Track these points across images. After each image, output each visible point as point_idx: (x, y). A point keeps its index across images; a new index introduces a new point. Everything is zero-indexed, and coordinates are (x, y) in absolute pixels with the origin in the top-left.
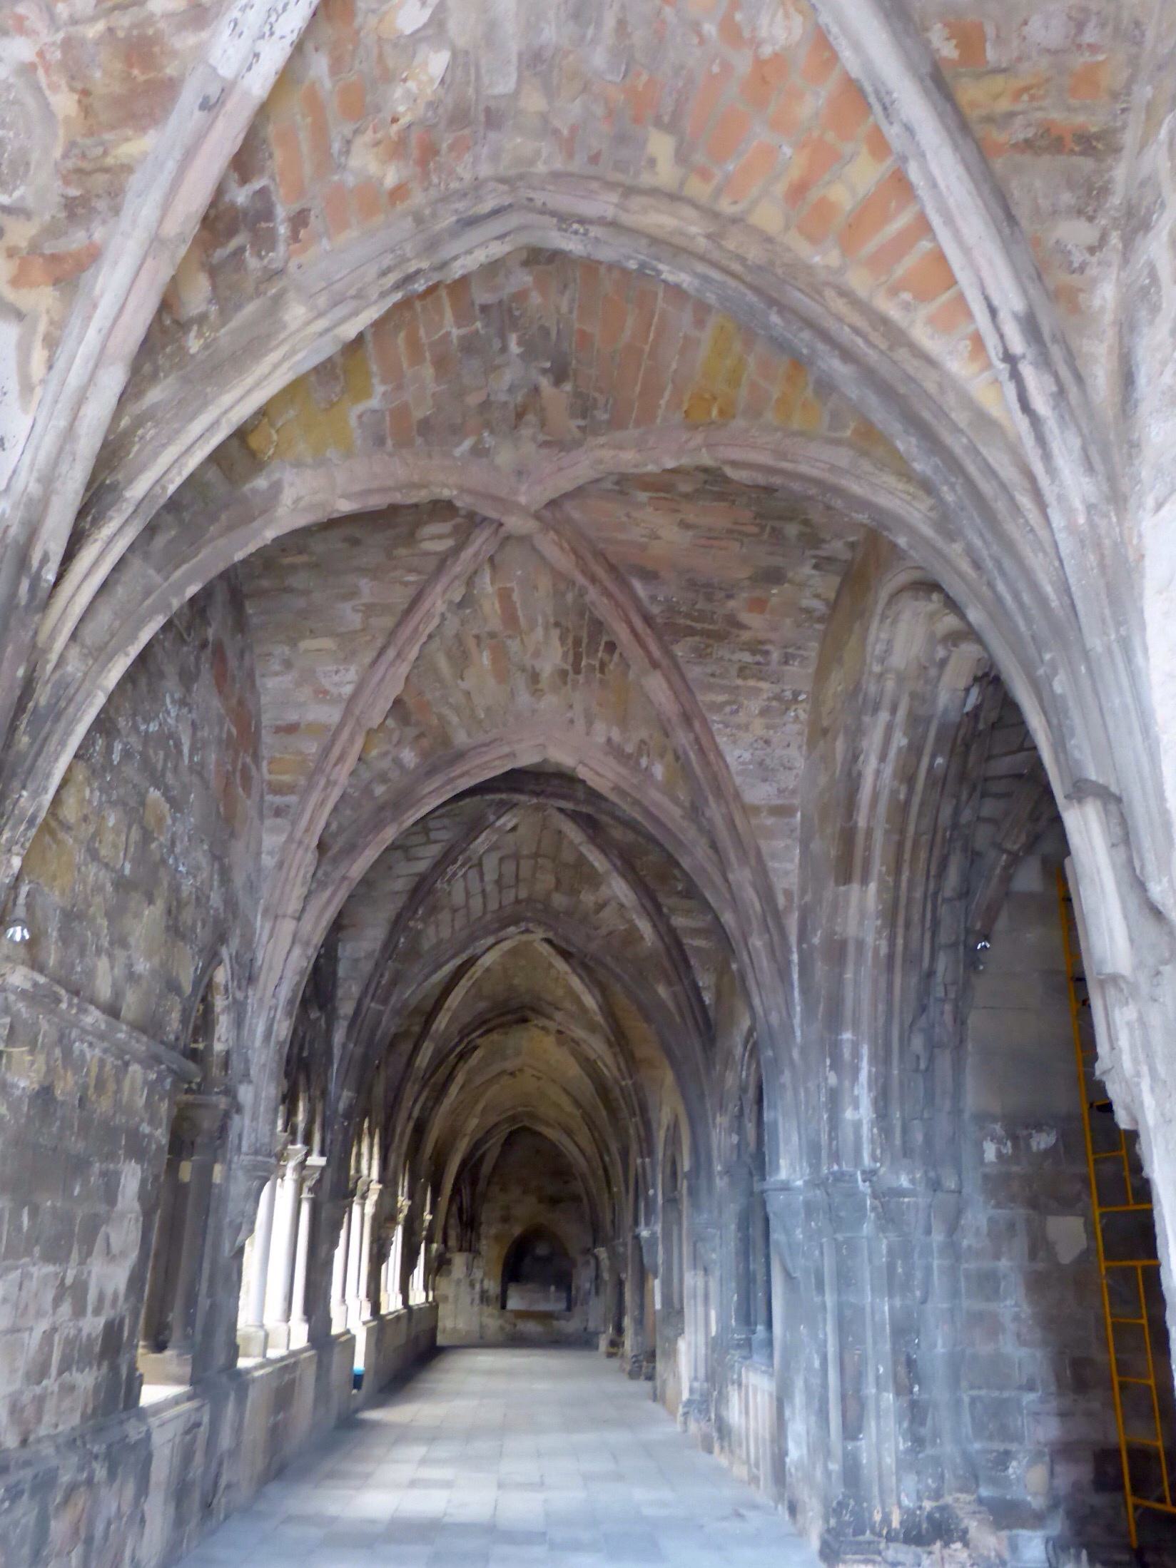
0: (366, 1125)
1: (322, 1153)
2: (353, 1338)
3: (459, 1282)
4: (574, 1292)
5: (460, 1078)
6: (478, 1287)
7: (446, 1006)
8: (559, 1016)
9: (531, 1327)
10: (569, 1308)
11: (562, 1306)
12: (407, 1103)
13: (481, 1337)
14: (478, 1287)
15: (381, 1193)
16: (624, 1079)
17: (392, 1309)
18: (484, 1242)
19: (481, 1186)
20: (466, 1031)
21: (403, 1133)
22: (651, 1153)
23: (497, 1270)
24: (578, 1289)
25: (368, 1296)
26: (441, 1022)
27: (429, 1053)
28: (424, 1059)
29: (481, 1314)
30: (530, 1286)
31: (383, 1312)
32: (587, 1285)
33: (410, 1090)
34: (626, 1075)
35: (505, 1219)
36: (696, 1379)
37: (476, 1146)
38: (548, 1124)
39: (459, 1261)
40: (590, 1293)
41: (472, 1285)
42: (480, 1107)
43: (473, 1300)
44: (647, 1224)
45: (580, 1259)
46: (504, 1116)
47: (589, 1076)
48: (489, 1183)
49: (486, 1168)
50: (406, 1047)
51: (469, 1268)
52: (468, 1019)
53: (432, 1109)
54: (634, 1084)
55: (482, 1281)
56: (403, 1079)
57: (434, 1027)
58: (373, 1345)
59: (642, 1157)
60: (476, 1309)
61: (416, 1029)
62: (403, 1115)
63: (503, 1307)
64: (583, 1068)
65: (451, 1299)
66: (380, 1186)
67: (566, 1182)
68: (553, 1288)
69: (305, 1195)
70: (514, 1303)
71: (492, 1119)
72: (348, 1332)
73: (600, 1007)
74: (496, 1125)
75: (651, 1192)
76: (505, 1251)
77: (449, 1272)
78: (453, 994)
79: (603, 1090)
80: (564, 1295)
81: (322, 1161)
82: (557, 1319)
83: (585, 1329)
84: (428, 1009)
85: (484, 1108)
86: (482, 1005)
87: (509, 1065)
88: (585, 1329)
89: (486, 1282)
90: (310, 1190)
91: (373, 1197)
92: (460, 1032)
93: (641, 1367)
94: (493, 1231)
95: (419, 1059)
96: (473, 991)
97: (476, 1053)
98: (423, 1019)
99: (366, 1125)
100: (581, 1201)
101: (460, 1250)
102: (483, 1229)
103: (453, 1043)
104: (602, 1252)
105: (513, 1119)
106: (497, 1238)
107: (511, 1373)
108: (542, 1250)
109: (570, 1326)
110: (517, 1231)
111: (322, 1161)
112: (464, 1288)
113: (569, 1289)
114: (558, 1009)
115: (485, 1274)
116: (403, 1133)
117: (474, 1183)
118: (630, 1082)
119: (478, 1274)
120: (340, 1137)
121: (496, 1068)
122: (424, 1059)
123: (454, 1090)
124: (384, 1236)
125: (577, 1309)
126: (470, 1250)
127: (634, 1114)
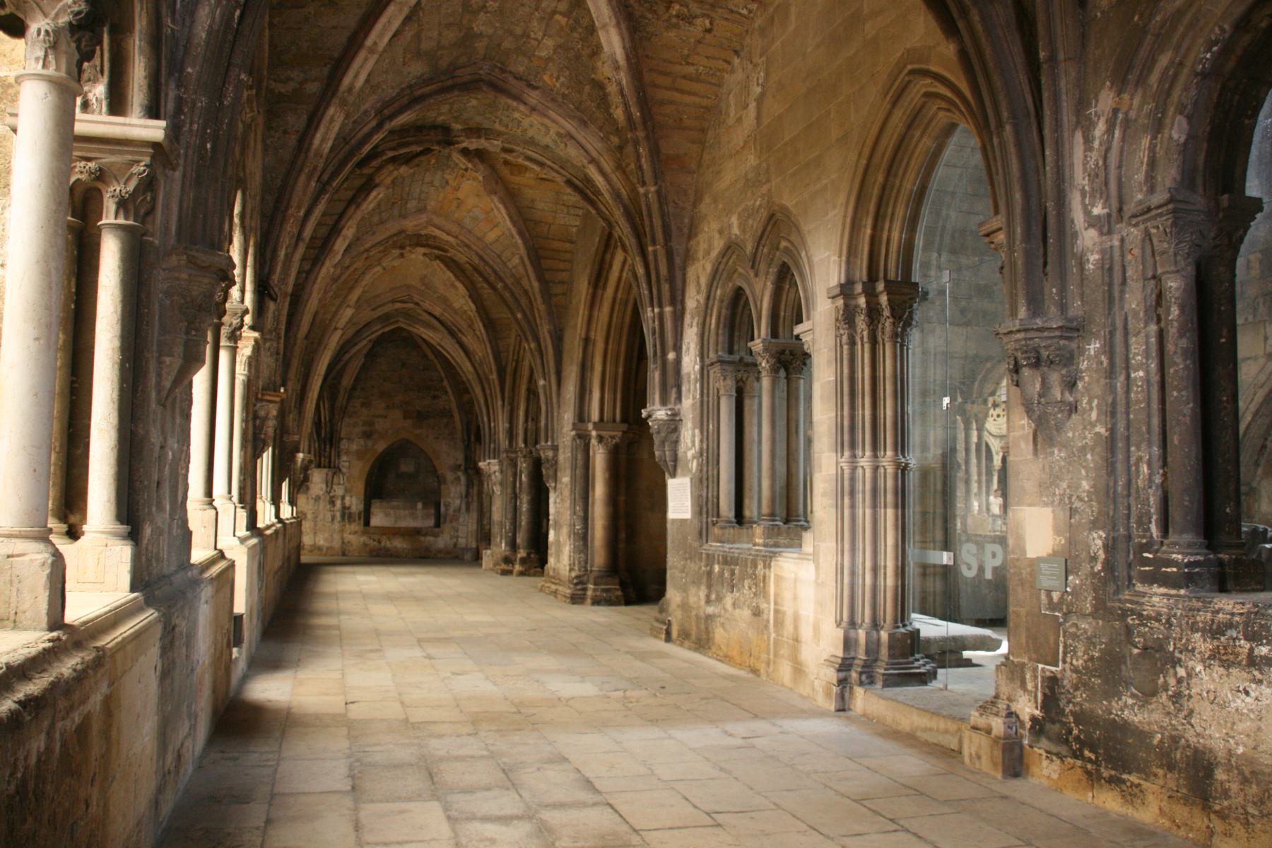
0: (237, 210)
1: (153, 111)
2: (232, 565)
3: (317, 499)
4: (443, 509)
5: (349, 232)
6: (338, 503)
7: (369, 42)
8: (533, 97)
9: (398, 544)
10: (438, 525)
11: (431, 522)
12: (295, 213)
13: (344, 554)
14: (338, 503)
15: (257, 347)
16: (644, 184)
17: (268, 522)
18: (344, 458)
19: (341, 399)
20: (386, 112)
21: (289, 258)
22: (678, 300)
23: (360, 487)
24: (447, 506)
25: (241, 500)
26: (359, 73)
27: (336, 127)
28: (324, 139)
29: (342, 531)
30: (395, 503)
31: (260, 525)
32: (458, 502)
33: (303, 188)
34: (648, 175)
35: (367, 435)
36: (852, 624)
37: (344, 348)
38: (428, 326)
39: (318, 478)
40: (460, 509)
41: (332, 503)
42: (354, 297)
43: (333, 518)
44: (664, 402)
45: (450, 476)
46: (379, 313)
47: (521, 233)
48: (349, 399)
49: (347, 381)
50: (295, 121)
51: (329, 484)
52: (392, 93)
53: (309, 272)
54: (658, 192)
55: (343, 498)
56: (292, 169)
57: (347, 81)
58: (255, 576)
59: (660, 306)
60: (337, 526)
61: (313, 88)
62: (290, 227)
63: (367, 523)
64: (514, 223)
65: (309, 516)
66: (256, 335)
67: (435, 397)
68: (420, 506)
69: (109, 216)
70: (377, 520)
71: (368, 315)
72: (222, 555)
73: (628, 58)
74: (368, 325)
75: (671, 356)
76: (367, 469)
77: (308, 488)
78: (383, 20)
79: (538, 253)
80: (432, 511)
81: (155, 130)
82: (425, 535)
83: (455, 545)
84: (336, 55)
85: (359, 299)
86: (417, 69)
87: (410, 224)
88: (455, 545)
89: (347, 499)
90: (122, 205)
91: (246, 350)
92: (379, 112)
93: (585, 589)
94: (354, 447)
95: (318, 136)
96: (409, 34)
97: (374, 194)
98: (326, 71)
99: (237, 210)
100: (452, 416)
101: (319, 466)
102: (344, 445)
103: (366, 130)
104: (490, 466)
105: (386, 318)
106: (360, 455)
107: (417, 599)
108: (407, 467)
109: (443, 541)
110: (381, 446)
111: (155, 130)
112: (323, 505)
113: (437, 506)
114: (530, 86)
115: (346, 490)
116: (289, 258)
117: (333, 398)
118: (653, 189)
119: (339, 491)
120: (202, 102)
121: (394, 227)
122: (324, 139)
123: (340, 245)
124: (262, 413)
125: (447, 528)
126: (329, 467)
127: (654, 243)
